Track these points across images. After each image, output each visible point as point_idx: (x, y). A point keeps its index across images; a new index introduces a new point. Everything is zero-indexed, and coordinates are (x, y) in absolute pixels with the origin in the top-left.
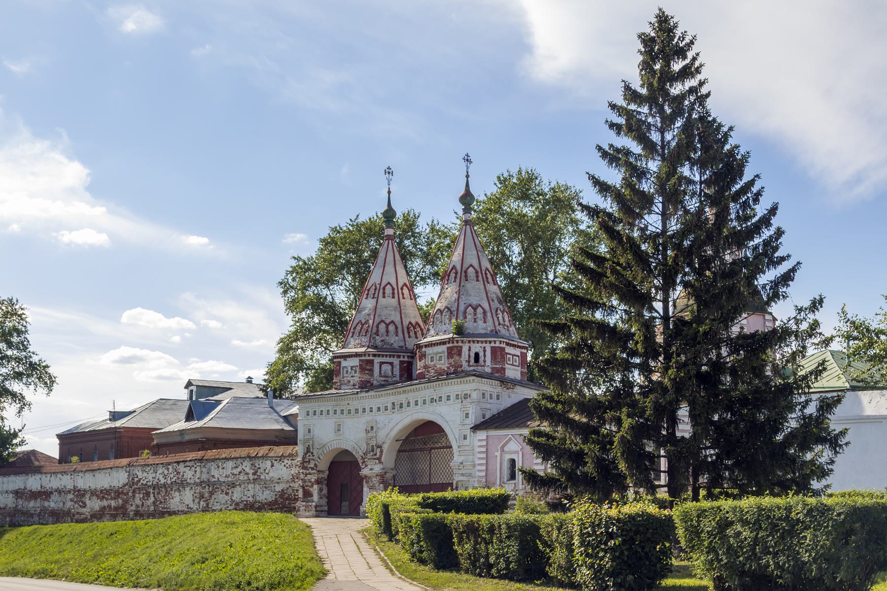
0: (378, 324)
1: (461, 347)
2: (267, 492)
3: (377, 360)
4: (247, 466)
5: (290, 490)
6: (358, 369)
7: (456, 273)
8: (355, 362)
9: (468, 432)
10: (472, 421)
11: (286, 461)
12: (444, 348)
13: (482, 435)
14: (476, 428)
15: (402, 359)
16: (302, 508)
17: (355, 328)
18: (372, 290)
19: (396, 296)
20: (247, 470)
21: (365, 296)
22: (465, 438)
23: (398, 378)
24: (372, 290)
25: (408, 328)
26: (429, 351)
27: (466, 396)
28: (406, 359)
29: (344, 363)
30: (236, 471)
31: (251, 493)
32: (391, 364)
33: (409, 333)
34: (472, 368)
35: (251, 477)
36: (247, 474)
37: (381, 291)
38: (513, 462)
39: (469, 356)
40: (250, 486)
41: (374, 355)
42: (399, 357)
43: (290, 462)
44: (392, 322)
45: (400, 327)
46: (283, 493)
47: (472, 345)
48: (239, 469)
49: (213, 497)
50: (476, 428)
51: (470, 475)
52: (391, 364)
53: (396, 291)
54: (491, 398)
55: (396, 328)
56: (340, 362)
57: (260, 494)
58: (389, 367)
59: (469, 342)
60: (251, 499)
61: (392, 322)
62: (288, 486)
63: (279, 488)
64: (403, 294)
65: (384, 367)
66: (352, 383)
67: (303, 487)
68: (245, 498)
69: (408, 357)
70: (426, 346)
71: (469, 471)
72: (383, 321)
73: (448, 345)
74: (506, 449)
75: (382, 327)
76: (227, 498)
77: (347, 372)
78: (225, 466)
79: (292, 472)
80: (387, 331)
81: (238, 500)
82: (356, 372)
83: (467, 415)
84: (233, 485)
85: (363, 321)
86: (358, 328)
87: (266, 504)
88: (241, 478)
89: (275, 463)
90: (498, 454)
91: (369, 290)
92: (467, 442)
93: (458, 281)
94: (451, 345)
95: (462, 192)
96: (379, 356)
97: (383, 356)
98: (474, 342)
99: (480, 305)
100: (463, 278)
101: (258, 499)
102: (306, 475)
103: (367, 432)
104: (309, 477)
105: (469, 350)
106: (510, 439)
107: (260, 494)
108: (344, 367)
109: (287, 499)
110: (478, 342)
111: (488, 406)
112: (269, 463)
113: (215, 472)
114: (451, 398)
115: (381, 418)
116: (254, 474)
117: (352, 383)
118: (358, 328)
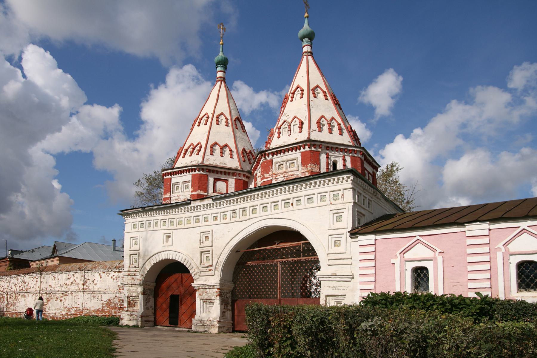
2: (94, 301)
4: (78, 276)
6: (190, 184)
8: (188, 177)
10: (347, 221)
11: (112, 273)
13: (370, 239)
14: (354, 234)
17: (186, 150)
18: (205, 118)
20: (78, 281)
22: (337, 244)
27: (336, 197)
30: (69, 282)
31: (80, 301)
35: (81, 287)
36: (78, 284)
41: (209, 171)
50: (354, 234)
57: (89, 303)
62: (114, 295)
68: (76, 305)
74: (408, 256)
79: (119, 284)
81: (69, 307)
82: (187, 187)
83: (339, 219)
85: (195, 145)
86: (190, 150)
91: (201, 119)
96: (213, 171)
101: (86, 306)
107: (89, 303)
112: (97, 275)
113: (51, 282)
118: (190, 150)
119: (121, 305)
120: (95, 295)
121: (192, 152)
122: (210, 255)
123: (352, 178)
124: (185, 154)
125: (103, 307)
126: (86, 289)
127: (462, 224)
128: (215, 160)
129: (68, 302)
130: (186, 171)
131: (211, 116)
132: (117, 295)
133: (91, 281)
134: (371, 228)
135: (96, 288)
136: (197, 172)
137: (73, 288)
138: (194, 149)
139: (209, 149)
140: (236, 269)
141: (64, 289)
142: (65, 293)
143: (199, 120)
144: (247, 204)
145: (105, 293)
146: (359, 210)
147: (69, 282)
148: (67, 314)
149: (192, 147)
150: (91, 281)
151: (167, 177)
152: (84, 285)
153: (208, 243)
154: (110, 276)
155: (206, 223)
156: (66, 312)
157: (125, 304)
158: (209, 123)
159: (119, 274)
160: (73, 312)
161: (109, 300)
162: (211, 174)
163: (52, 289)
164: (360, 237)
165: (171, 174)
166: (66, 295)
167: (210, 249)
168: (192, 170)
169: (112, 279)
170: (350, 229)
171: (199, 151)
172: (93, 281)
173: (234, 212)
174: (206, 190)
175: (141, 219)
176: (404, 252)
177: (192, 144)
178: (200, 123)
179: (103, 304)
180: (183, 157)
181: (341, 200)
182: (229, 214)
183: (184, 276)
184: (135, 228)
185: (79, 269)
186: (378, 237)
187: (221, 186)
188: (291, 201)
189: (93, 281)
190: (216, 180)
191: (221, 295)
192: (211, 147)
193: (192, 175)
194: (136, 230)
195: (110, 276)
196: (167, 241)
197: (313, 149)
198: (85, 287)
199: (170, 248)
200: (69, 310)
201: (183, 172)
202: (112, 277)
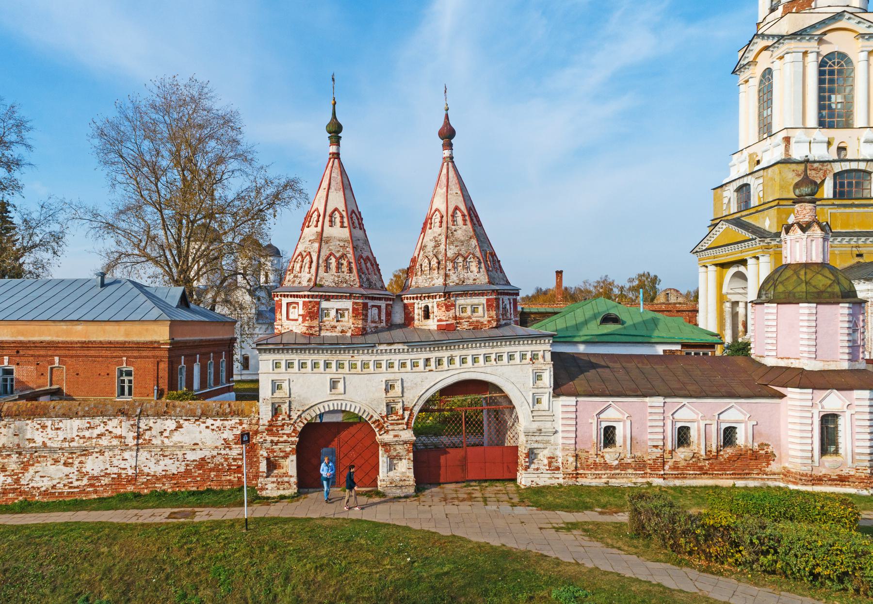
3: (371, 303)
5: (219, 460)
11: (209, 421)
16: (269, 486)
23: (384, 324)
26: (461, 301)
29: (324, 304)
32: (379, 307)
35: (131, 442)
40: (127, 455)
43: (218, 423)
46: (202, 463)
49: (31, 470)
51: (548, 442)
56: (319, 303)
60: (130, 472)
62: (215, 453)
65: (375, 311)
66: (339, 329)
67: (268, 459)
68: (115, 470)
71: (546, 438)
76: (67, 470)
79: (225, 436)
84: (85, 452)
87: (165, 476)
88: (104, 442)
89: (186, 424)
93: (468, 222)
95: (440, 123)
101: (146, 470)
102: (276, 444)
103: (387, 391)
104: (280, 446)
106: (609, 406)
107: (151, 464)
108: (323, 310)
109: (211, 470)
112: (170, 424)
115: (410, 377)
117: (339, 329)
120: (166, 453)
126: (142, 444)
129: (94, 465)
130: (346, 297)
132: (223, 452)
133: (154, 432)
143: (327, 218)
156: (85, 481)
159: (225, 422)
160: (105, 481)
161: (203, 459)
166: (84, 455)
169: (209, 431)
172: (161, 433)
173: (428, 360)
179: (187, 465)
181: (541, 360)
182: (421, 363)
189: (161, 433)
198: (141, 441)
199: (341, 397)
201: (341, 297)
202: (207, 427)
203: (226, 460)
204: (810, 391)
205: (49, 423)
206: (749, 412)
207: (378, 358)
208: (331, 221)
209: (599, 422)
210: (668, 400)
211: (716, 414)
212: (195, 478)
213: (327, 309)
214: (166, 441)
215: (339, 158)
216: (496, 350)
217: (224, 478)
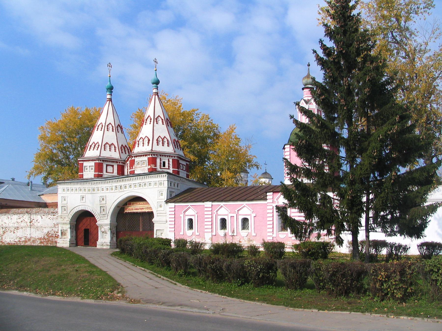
0: (105, 144)
1: (156, 158)
2: (38, 232)
4: (26, 217)
5: (52, 232)
7: (151, 119)
8: (92, 163)
9: (163, 204)
11: (50, 216)
12: (146, 158)
13: (172, 205)
14: (167, 202)
15: (119, 164)
17: (91, 146)
18: (100, 126)
19: (114, 131)
20: (26, 220)
21: (96, 129)
22: (161, 206)
24: (100, 126)
25: (121, 148)
27: (161, 184)
28: (121, 164)
30: (19, 221)
33: (122, 150)
34: (161, 170)
35: (29, 224)
37: (106, 127)
38: (191, 221)
39: (160, 163)
41: (103, 161)
42: (117, 162)
44: (112, 144)
45: (117, 146)
47: (162, 158)
48: (21, 220)
50: (167, 202)
52: (113, 166)
53: (114, 128)
54: (174, 186)
55: (115, 147)
58: (111, 168)
59: (160, 155)
61: (112, 144)
62: (51, 229)
63: (46, 231)
64: (118, 130)
69: (122, 163)
70: (135, 157)
72: (107, 143)
73: (148, 156)
74: (187, 213)
75: (108, 146)
77: (87, 169)
78: (12, 217)
80: (110, 149)
82: (92, 169)
84: (17, 228)
86: (93, 146)
90: (182, 215)
91: (98, 126)
92: (162, 209)
94: (150, 156)
96: (106, 161)
97: (108, 161)
98: (163, 155)
99: (165, 137)
100: (155, 122)
105: (160, 160)
110: (165, 156)
111: (173, 190)
114: (152, 184)
116: (30, 222)
119: (55, 235)
121: (94, 148)
122: (105, 208)
123: (167, 176)
124: (90, 148)
125: (44, 236)
127: (203, 202)
128: (107, 154)
130: (92, 160)
131: (104, 125)
133: (35, 220)
134: (174, 200)
135: (39, 225)
136: (97, 162)
137: (23, 224)
138: (95, 146)
139: (103, 147)
140: (117, 215)
141: (16, 225)
142: (17, 228)
144: (122, 183)
145: (45, 228)
146: (171, 190)
147: (19, 221)
148: (19, 241)
149: (94, 144)
150: (35, 220)
151: (81, 162)
152: (30, 222)
153: (104, 202)
154: (48, 218)
155: (103, 192)
157: (60, 234)
158: (103, 129)
160: (23, 239)
161: (48, 232)
162: (105, 162)
163: (7, 225)
164: (170, 204)
165: (83, 161)
167: (105, 205)
168: (94, 160)
170: (166, 200)
171: (98, 148)
174: (102, 171)
175: (67, 187)
176: (185, 212)
177: (94, 143)
178: (98, 129)
180: (89, 150)
183: (92, 218)
184: (64, 191)
185: (27, 212)
186: (177, 204)
187: (110, 169)
188: (142, 184)
190: (107, 165)
191: (110, 229)
192: (104, 146)
193: (95, 163)
194: (65, 192)
195: (48, 218)
196: (82, 200)
197: (153, 158)
198: (31, 224)
200: (20, 238)
201: (90, 160)
203: (55, 232)
204: (272, 193)
205: (9, 216)
206: (252, 209)
207: (98, 186)
208: (98, 129)
209: (185, 216)
210: (215, 203)
211: (236, 211)
212: (46, 239)
213: (86, 166)
214: (38, 224)
215: (111, 101)
216: (143, 181)
217: (54, 240)
